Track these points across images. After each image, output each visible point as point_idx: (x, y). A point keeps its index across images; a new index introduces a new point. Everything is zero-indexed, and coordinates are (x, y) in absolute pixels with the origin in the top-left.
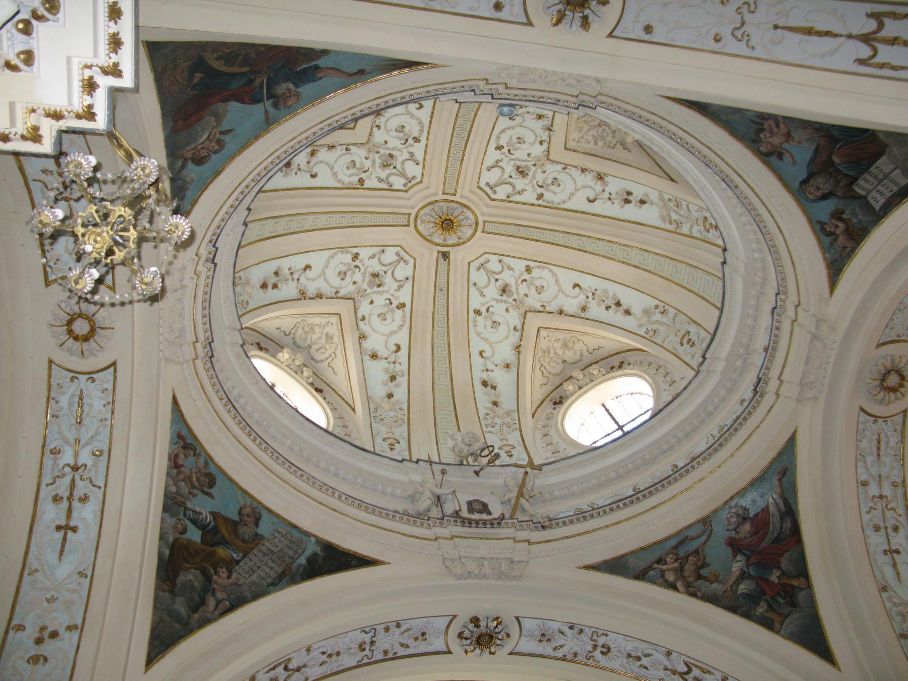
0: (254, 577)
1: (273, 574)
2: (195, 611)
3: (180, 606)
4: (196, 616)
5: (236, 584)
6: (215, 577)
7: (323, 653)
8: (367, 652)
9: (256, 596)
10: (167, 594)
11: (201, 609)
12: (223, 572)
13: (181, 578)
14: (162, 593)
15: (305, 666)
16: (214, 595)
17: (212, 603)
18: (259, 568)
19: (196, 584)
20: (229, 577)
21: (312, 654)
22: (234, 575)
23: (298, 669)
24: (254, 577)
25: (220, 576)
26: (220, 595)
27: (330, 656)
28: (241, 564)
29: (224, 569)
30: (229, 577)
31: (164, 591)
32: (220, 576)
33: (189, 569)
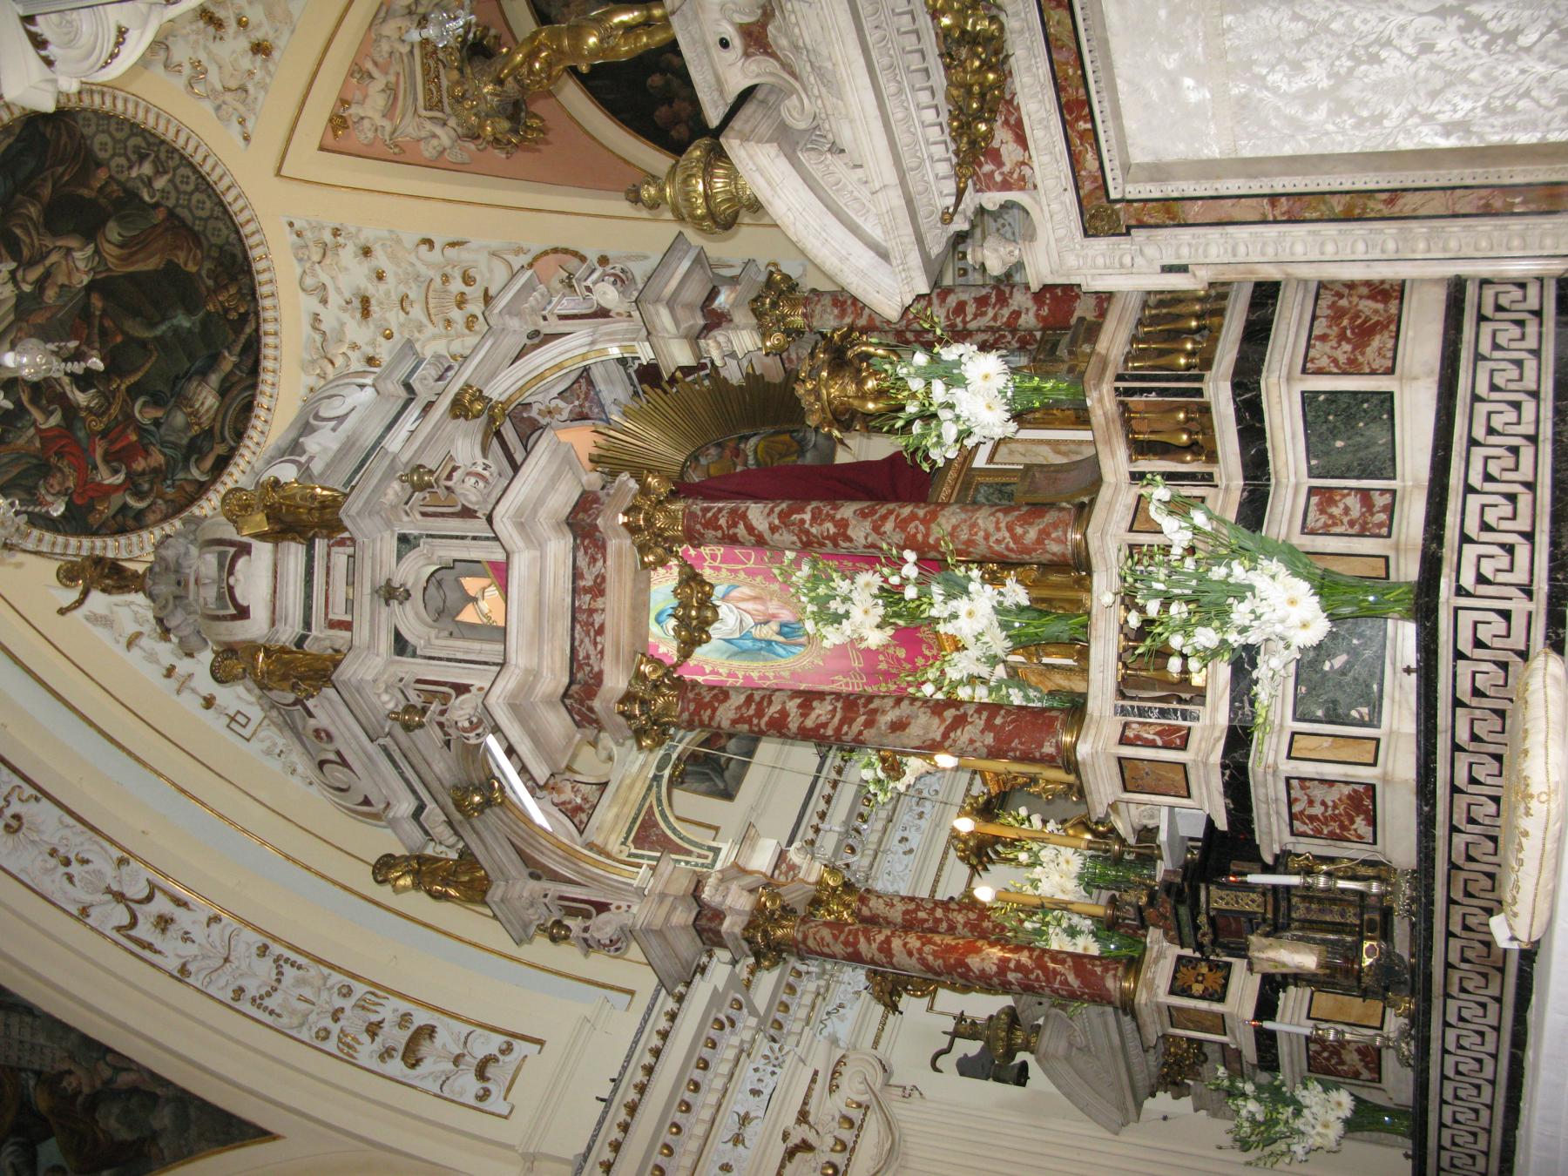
0: (41, 1039)
1: (14, 1020)
2: (154, 1097)
3: (163, 1118)
4: (158, 1091)
5: (72, 1057)
6: (86, 1090)
7: (70, 878)
8: (16, 807)
9: (67, 1029)
10: (162, 1144)
11: (143, 1087)
12: (69, 1083)
13: (124, 1135)
14: (166, 1152)
15: (109, 890)
16: (111, 1081)
17: (125, 1079)
18: (21, 1042)
19: (116, 1110)
20: (70, 1072)
21: (87, 898)
22: (65, 1067)
23: (120, 897)
24: (42, 1041)
25: (80, 1084)
26: (107, 1073)
27: (67, 862)
28: (37, 1067)
29: (65, 1084)
30: (70, 1072)
31: (161, 1151)
32: (80, 1084)
33: (104, 1132)
